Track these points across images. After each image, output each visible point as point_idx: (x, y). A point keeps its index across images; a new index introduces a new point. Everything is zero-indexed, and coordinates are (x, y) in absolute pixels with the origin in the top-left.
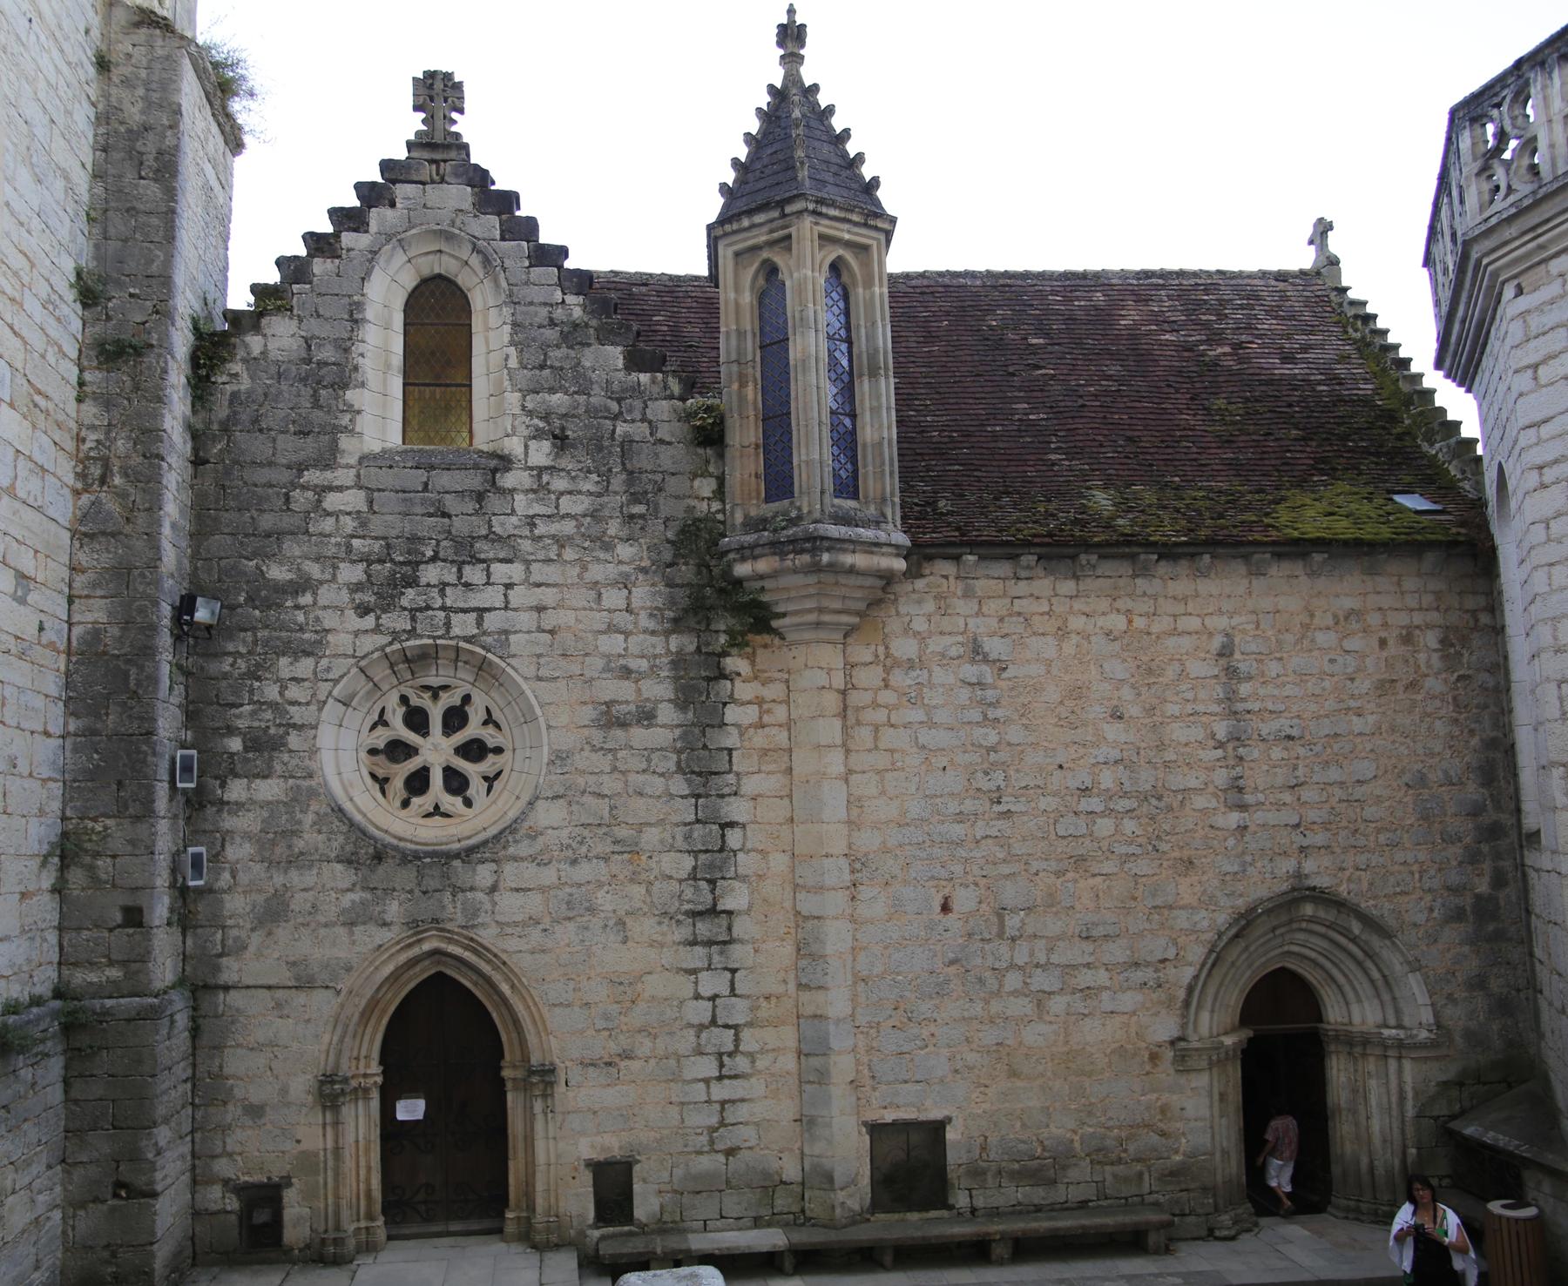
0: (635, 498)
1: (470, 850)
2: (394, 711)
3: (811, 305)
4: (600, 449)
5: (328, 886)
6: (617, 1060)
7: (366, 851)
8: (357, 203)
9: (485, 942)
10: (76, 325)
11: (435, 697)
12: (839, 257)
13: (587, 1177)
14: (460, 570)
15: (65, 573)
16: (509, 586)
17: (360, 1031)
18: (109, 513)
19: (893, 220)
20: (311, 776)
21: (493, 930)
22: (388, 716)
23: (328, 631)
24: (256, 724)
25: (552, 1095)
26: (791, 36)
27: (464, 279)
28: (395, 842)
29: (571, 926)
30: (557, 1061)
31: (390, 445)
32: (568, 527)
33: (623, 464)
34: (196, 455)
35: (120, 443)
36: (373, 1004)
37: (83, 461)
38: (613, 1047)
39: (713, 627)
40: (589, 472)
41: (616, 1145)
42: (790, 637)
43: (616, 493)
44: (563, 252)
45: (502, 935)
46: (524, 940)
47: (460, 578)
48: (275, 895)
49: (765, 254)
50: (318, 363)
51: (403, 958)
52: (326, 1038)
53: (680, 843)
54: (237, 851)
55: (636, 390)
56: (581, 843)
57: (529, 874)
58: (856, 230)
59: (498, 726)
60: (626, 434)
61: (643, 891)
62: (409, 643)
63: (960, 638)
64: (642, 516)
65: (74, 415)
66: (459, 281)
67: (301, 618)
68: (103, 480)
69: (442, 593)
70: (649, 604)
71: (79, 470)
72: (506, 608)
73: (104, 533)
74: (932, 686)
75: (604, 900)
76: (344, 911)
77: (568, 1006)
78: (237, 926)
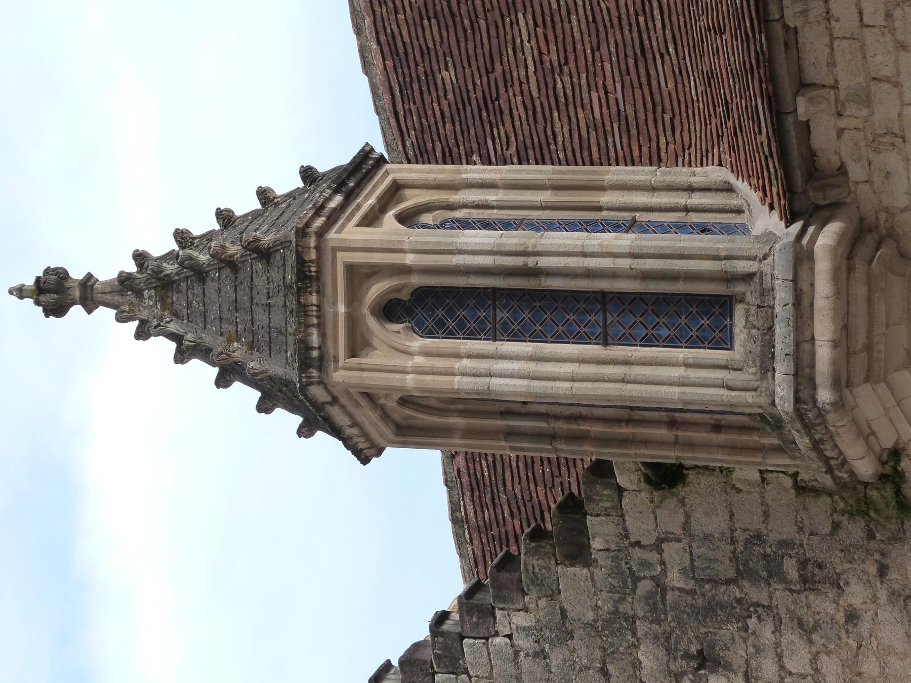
0: (775, 573)
33: (728, 582)
40: (746, 628)
55: (617, 554)
60: (684, 572)
64: (803, 564)
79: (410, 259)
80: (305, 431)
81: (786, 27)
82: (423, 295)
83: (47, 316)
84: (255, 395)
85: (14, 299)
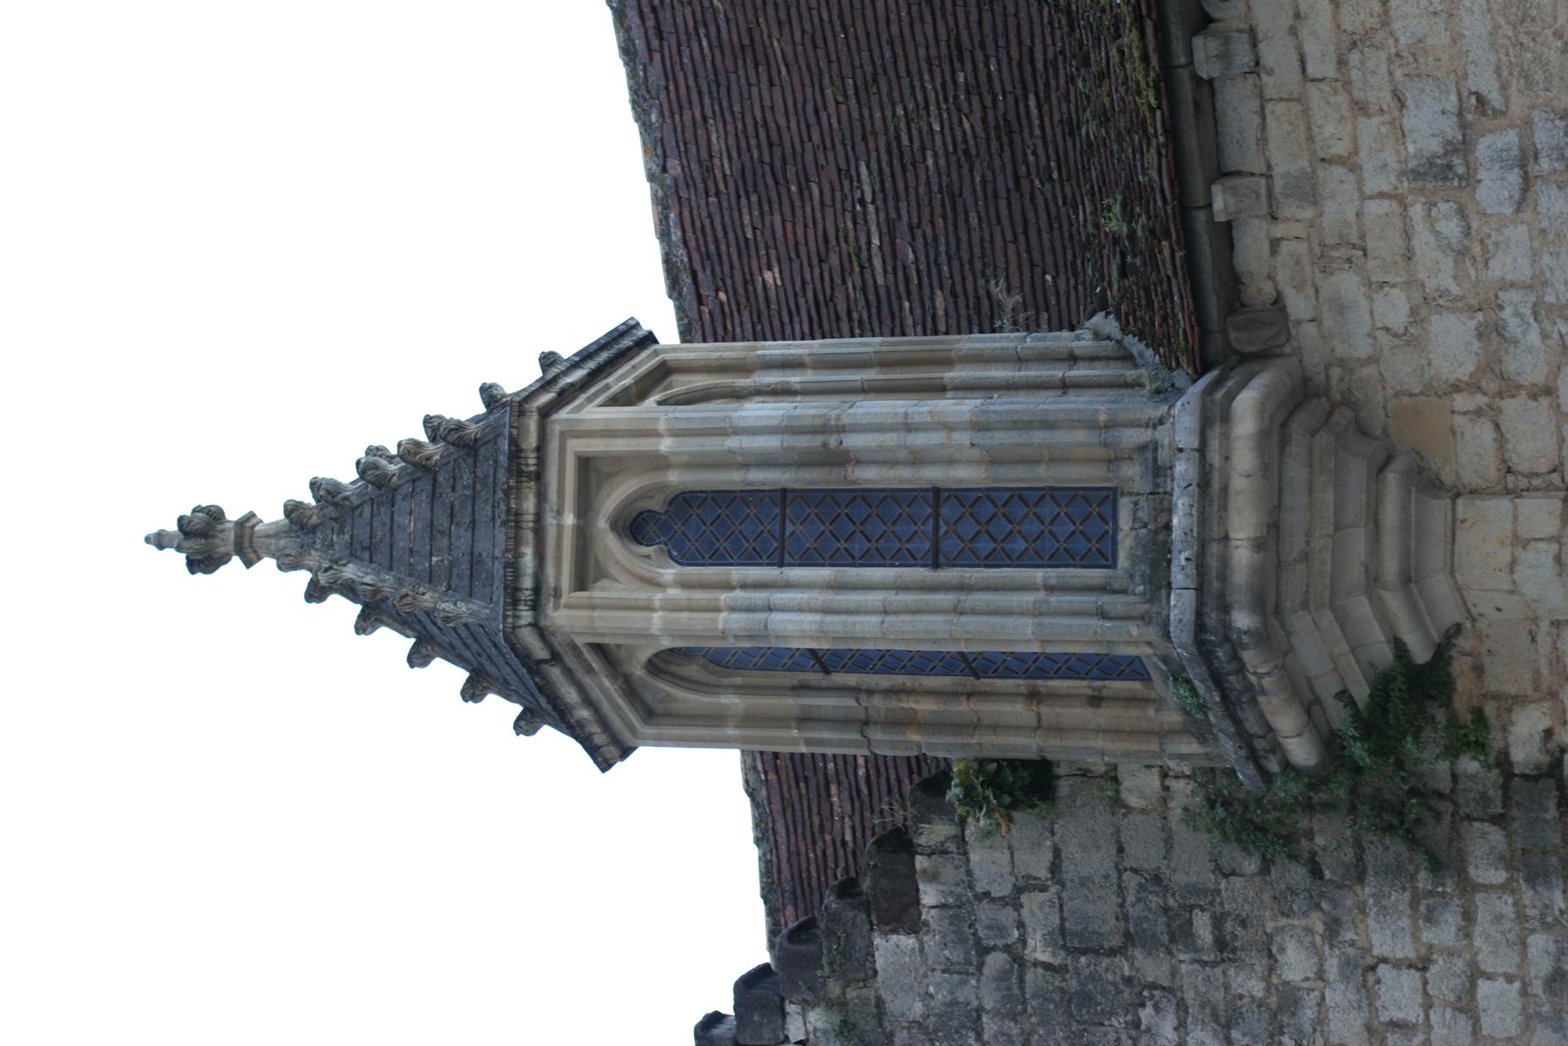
0: (1181, 934)
4: (1086, 998)
33: (1112, 952)
39: (1445, 785)
40: (1136, 1024)
42: (1450, 614)
43: (1174, 973)
55: (957, 912)
63: (1417, 211)
64: (1218, 922)
70: (1405, 922)
74: (1538, 283)
79: (665, 445)
80: (526, 725)
81: (1196, 78)
82: (685, 501)
83: (192, 572)
84: (461, 675)
85: (152, 548)
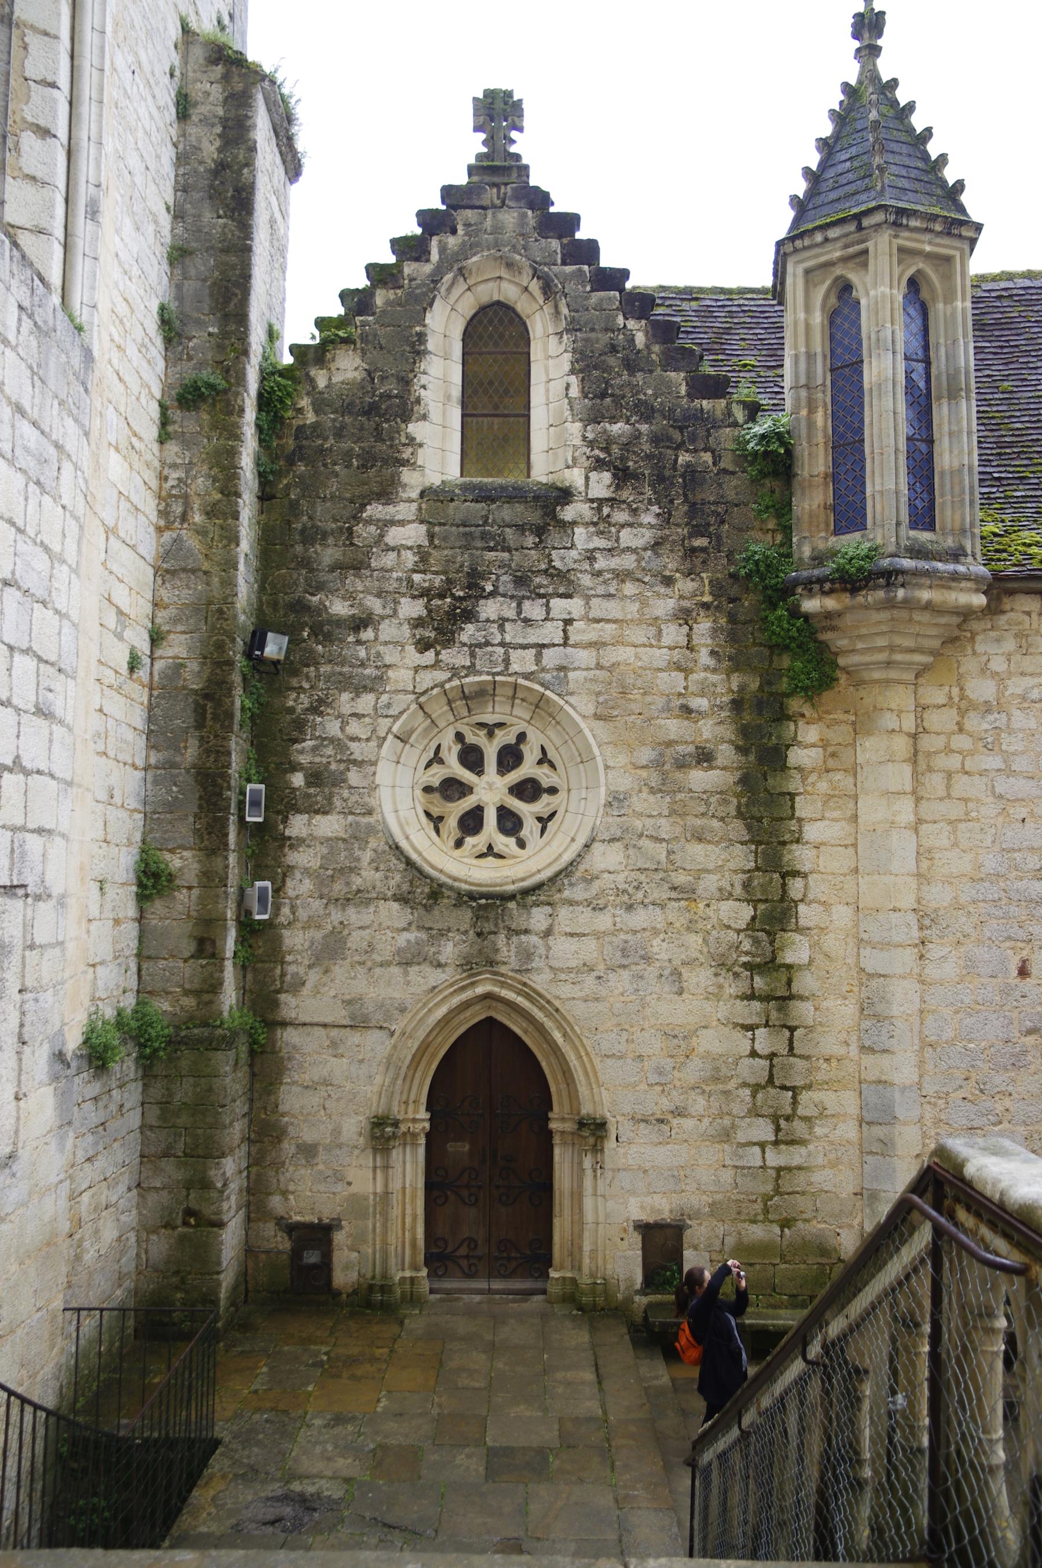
1: (526, 892)
2: (450, 749)
3: (889, 325)
5: (384, 925)
6: (669, 1117)
7: (422, 890)
8: (419, 231)
9: (538, 988)
10: (161, 364)
11: (491, 735)
12: (919, 271)
13: (637, 1239)
14: (519, 605)
15: (148, 608)
16: (568, 622)
17: (410, 1074)
18: (189, 550)
19: (979, 227)
20: (370, 813)
21: (547, 975)
22: (444, 754)
23: (388, 667)
24: (317, 760)
25: (602, 1150)
26: (869, 26)
27: (523, 306)
28: (450, 881)
29: (625, 974)
30: (608, 1115)
31: (450, 478)
32: (628, 562)
34: (263, 491)
35: (200, 480)
36: (424, 1047)
37: (164, 499)
38: (665, 1104)
40: (650, 502)
41: (667, 1208)
43: (677, 525)
44: (625, 274)
45: (555, 981)
46: (577, 987)
47: (519, 613)
48: (332, 932)
49: (838, 271)
50: (381, 396)
51: (456, 1001)
52: (378, 1079)
53: (738, 890)
54: (299, 887)
56: (637, 888)
57: (584, 919)
58: (938, 240)
59: (553, 766)
61: (700, 941)
62: (467, 680)
64: (704, 550)
65: (157, 454)
66: (519, 308)
67: (362, 654)
68: (184, 518)
69: (502, 628)
71: (161, 508)
72: (565, 644)
73: (184, 570)
75: (658, 947)
76: (399, 951)
77: (621, 1058)
78: (295, 962)
